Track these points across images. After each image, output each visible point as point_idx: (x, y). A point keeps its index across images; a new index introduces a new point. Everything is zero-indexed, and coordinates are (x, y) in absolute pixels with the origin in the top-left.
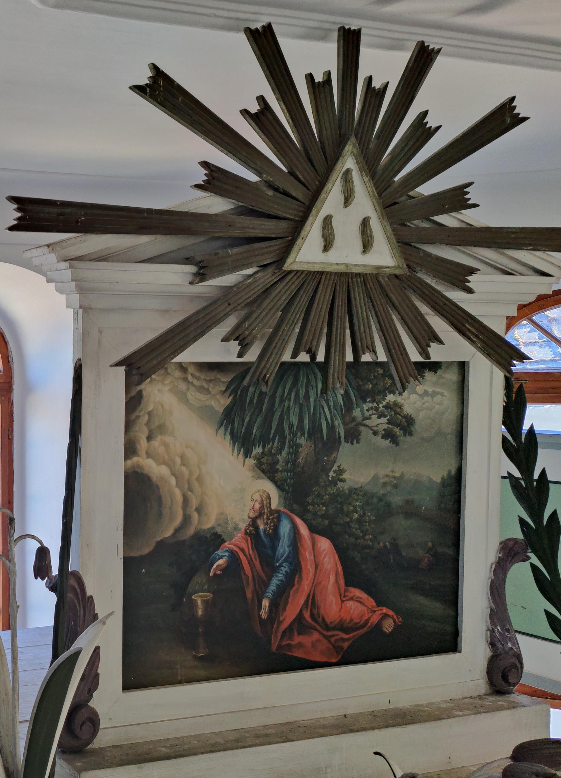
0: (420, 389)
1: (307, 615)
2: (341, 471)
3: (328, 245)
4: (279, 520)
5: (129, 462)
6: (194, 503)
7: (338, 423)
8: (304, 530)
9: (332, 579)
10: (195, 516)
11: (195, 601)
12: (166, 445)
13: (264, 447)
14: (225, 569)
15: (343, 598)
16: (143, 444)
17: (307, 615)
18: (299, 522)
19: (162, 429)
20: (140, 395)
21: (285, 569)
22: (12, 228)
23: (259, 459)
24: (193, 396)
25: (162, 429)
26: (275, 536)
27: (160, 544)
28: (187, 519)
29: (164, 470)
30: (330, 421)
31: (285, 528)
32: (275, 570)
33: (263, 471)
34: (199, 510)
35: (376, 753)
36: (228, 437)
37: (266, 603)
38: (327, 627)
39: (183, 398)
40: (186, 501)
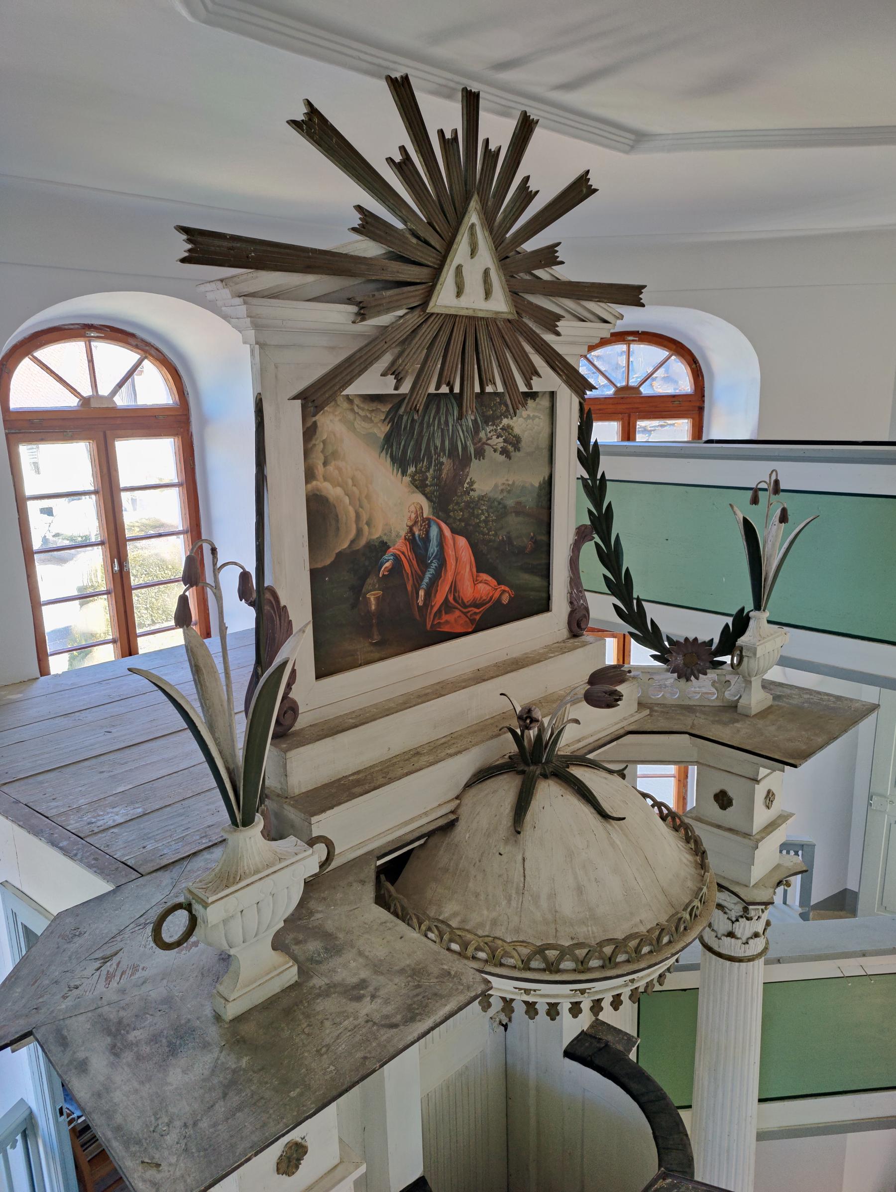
0: (525, 413)
1: (451, 599)
2: (472, 483)
4: (429, 526)
5: (309, 486)
6: (365, 517)
7: (469, 443)
9: (468, 569)
10: (366, 528)
11: (369, 598)
12: (339, 469)
13: (416, 467)
14: (391, 570)
15: (475, 582)
16: (320, 470)
17: (451, 599)
18: (444, 526)
19: (335, 455)
21: (435, 565)
22: (184, 260)
23: (413, 476)
24: (360, 425)
25: (335, 455)
26: (426, 539)
27: (339, 555)
28: (359, 532)
29: (339, 491)
30: (463, 442)
31: (434, 531)
32: (427, 566)
33: (416, 487)
34: (368, 524)
35: (502, 694)
36: (389, 459)
37: (422, 593)
38: (465, 606)
39: (351, 428)
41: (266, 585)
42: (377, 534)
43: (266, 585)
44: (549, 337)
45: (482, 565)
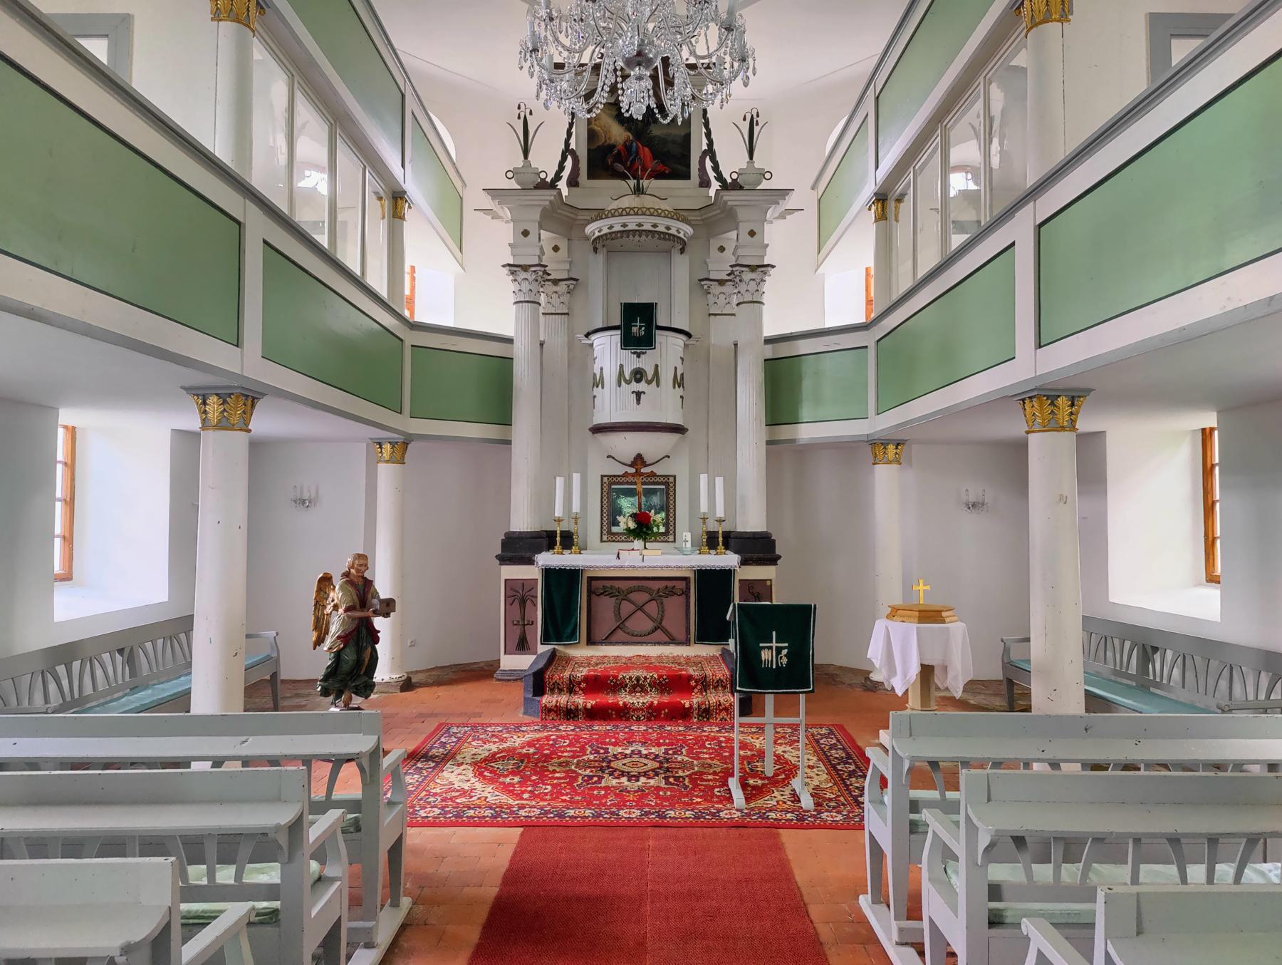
5: (591, 126)
6: (608, 137)
8: (640, 145)
9: (649, 158)
14: (617, 154)
26: (631, 146)
27: (598, 146)
28: (606, 141)
29: (599, 129)
31: (634, 144)
34: (609, 139)
37: (629, 163)
40: (605, 136)
41: (570, 148)
42: (612, 142)
43: (570, 148)
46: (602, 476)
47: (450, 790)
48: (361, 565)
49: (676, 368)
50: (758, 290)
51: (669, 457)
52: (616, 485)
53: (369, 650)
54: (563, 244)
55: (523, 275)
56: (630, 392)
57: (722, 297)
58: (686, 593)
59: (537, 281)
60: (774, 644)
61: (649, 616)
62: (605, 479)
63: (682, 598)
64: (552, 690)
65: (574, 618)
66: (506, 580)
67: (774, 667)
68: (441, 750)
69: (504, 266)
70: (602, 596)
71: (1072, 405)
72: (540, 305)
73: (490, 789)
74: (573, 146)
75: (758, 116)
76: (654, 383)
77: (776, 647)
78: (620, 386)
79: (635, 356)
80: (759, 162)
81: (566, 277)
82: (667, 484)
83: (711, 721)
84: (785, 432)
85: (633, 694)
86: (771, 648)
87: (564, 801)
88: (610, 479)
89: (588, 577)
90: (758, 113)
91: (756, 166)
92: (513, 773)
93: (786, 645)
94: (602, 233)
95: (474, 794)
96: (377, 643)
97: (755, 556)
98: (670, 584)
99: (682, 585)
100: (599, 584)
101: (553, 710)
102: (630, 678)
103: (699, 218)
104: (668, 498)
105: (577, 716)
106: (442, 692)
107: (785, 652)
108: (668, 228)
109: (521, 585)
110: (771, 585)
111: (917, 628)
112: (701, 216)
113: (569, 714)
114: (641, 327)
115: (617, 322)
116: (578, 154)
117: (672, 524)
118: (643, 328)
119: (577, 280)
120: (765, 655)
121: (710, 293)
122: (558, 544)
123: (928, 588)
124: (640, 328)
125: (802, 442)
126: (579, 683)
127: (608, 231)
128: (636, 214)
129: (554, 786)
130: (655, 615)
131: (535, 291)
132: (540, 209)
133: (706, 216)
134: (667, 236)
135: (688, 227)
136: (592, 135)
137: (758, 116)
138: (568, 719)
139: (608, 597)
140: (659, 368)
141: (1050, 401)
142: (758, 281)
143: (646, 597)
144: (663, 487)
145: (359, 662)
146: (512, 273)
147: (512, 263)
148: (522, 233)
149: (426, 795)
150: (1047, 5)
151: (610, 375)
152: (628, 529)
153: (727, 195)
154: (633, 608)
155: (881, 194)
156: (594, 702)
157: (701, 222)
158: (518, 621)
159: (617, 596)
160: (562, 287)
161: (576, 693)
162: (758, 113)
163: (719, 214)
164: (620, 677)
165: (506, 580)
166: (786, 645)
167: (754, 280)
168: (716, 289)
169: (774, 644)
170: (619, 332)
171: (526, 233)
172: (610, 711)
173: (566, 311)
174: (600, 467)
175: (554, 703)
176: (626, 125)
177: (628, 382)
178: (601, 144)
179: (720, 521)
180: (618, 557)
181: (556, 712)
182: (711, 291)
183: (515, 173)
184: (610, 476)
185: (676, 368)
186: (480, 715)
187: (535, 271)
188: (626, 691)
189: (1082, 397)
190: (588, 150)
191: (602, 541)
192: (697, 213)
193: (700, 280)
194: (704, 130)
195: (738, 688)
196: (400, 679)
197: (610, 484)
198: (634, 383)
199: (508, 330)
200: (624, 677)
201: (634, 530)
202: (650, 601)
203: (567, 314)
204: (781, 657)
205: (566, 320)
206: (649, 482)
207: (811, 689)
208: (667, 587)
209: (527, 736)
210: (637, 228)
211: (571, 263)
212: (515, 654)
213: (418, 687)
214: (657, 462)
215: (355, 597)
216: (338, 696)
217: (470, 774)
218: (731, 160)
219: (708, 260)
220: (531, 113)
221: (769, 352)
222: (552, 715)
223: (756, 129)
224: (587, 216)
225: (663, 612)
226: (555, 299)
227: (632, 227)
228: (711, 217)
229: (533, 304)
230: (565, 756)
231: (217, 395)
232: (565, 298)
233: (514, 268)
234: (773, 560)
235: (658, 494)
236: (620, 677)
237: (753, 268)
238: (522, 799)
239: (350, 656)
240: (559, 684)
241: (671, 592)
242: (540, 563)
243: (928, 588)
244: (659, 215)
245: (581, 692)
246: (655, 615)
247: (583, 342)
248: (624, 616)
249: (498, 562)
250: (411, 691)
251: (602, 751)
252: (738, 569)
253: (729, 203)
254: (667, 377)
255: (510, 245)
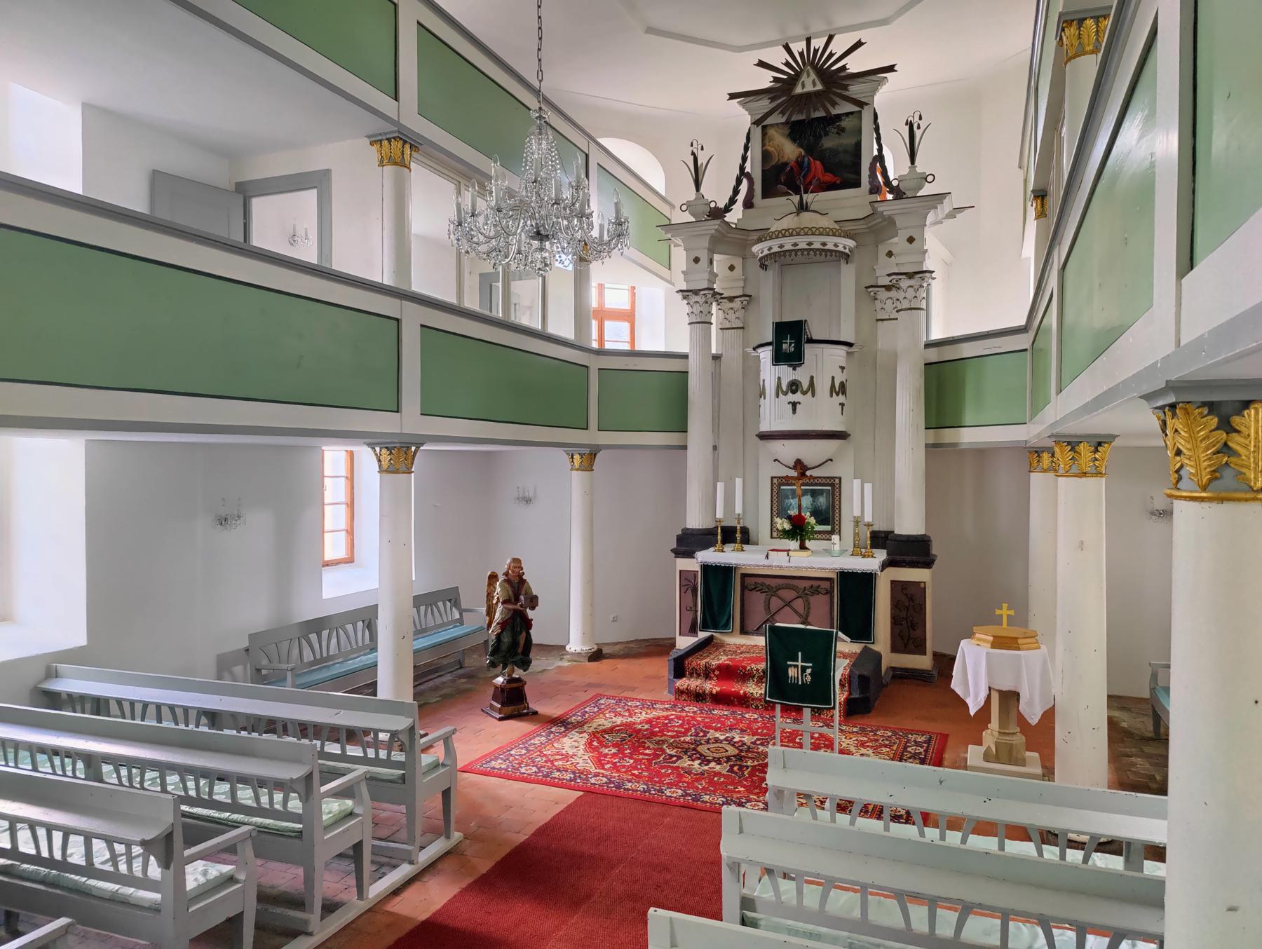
3: (803, 86)
4: (804, 158)
5: (764, 148)
6: (781, 155)
8: (812, 160)
15: (824, 176)
16: (767, 144)
20: (766, 133)
23: (798, 143)
24: (780, 131)
27: (772, 166)
28: (779, 160)
29: (773, 149)
31: (806, 159)
40: (779, 155)
42: (785, 159)
44: (846, 93)
45: (827, 169)
46: (772, 478)
47: (558, 754)
48: (515, 567)
49: (833, 378)
50: (916, 297)
51: (831, 460)
52: (784, 485)
53: (524, 634)
54: (738, 262)
55: (696, 298)
56: (787, 404)
57: (889, 302)
58: (830, 592)
59: (707, 303)
60: (800, 664)
61: (796, 612)
62: (775, 481)
63: (827, 598)
64: (691, 675)
65: (728, 611)
66: (680, 571)
67: (800, 683)
68: (580, 718)
69: (677, 292)
70: (754, 591)
71: (1096, 451)
72: (712, 324)
73: (586, 757)
74: (748, 169)
75: (920, 118)
76: (810, 393)
77: (802, 666)
78: (778, 397)
79: (791, 369)
80: (921, 167)
81: (740, 293)
82: (832, 485)
83: (822, 716)
84: (948, 436)
85: (760, 685)
86: (796, 666)
87: (634, 775)
88: (780, 480)
89: (742, 574)
90: (920, 115)
91: (919, 170)
92: (614, 746)
93: (811, 665)
94: (764, 254)
95: (571, 759)
96: (530, 629)
97: (908, 558)
98: (815, 583)
99: (826, 585)
100: (754, 580)
101: (684, 692)
102: (757, 670)
103: (865, 227)
104: (833, 499)
105: (705, 699)
106: (622, 665)
107: (809, 671)
108: (824, 244)
109: (693, 576)
110: (925, 588)
111: (987, 653)
112: (866, 224)
113: (698, 697)
114: (790, 344)
115: (770, 339)
116: (753, 176)
117: (837, 523)
118: (793, 345)
119: (750, 296)
120: (792, 672)
121: (877, 299)
122: (719, 542)
123: (1012, 613)
124: (790, 345)
125: (963, 447)
126: (714, 671)
127: (768, 252)
128: (791, 235)
129: (636, 761)
130: (801, 611)
131: (705, 312)
132: (708, 238)
133: (873, 223)
134: (824, 252)
135: (851, 241)
136: (766, 156)
137: (920, 118)
138: (697, 701)
139: (759, 592)
140: (815, 379)
141: (1069, 448)
142: (916, 287)
143: (792, 594)
144: (830, 488)
145: (514, 644)
146: (684, 298)
147: (685, 289)
148: (694, 260)
149: (538, 755)
150: (1080, 38)
151: (770, 387)
152: (784, 531)
153: (881, 206)
154: (781, 603)
155: (1040, 190)
156: (719, 689)
157: (868, 230)
158: (691, 608)
159: (767, 592)
160: (737, 304)
161: (710, 679)
162: (920, 115)
163: (881, 222)
164: (748, 668)
165: (680, 571)
166: (811, 665)
167: (912, 287)
168: (883, 294)
169: (800, 664)
170: (770, 348)
171: (697, 260)
172: (732, 698)
173: (741, 325)
174: (769, 470)
175: (686, 686)
176: (798, 141)
177: (785, 394)
178: (774, 163)
179: (869, 525)
180: (767, 557)
181: (687, 694)
182: (878, 297)
183: (689, 206)
184: (780, 478)
185: (833, 378)
186: (633, 689)
187: (704, 294)
188: (754, 681)
189: (1107, 443)
190: (763, 171)
191: (772, 537)
192: (862, 222)
193: (867, 288)
194: (875, 136)
195: (767, 699)
196: (590, 651)
197: (780, 485)
198: (790, 394)
199: (684, 348)
200: (752, 669)
201: (789, 531)
202: (796, 598)
203: (743, 328)
204: (806, 676)
205: (741, 333)
206: (820, 483)
207: (832, 706)
208: (812, 586)
209: (654, 713)
210: (793, 248)
211: (745, 281)
212: (688, 636)
213: (607, 658)
214: (820, 465)
215: (510, 593)
216: (504, 668)
217: (583, 741)
218: (896, 166)
219: (875, 267)
220: (702, 149)
221: (933, 355)
222: (685, 696)
223: (918, 133)
224: (755, 236)
225: (809, 608)
226: (731, 316)
227: (788, 247)
228: (875, 225)
229: (704, 324)
230: (667, 736)
231: (387, 448)
232: (740, 313)
233: (686, 294)
234: (928, 564)
235: (825, 494)
236: (748, 668)
237: (910, 275)
238: (604, 769)
239: (506, 639)
240: (696, 670)
241: (816, 591)
242: (700, 560)
243: (1012, 613)
244: (813, 234)
245: (715, 678)
246: (801, 611)
247: (752, 355)
248: (773, 608)
249: (673, 555)
250: (598, 661)
251: (701, 734)
252: (879, 573)
253: (885, 213)
254: (823, 386)
255: (683, 272)
